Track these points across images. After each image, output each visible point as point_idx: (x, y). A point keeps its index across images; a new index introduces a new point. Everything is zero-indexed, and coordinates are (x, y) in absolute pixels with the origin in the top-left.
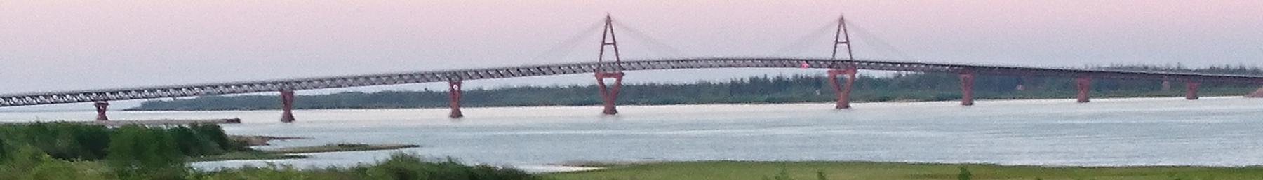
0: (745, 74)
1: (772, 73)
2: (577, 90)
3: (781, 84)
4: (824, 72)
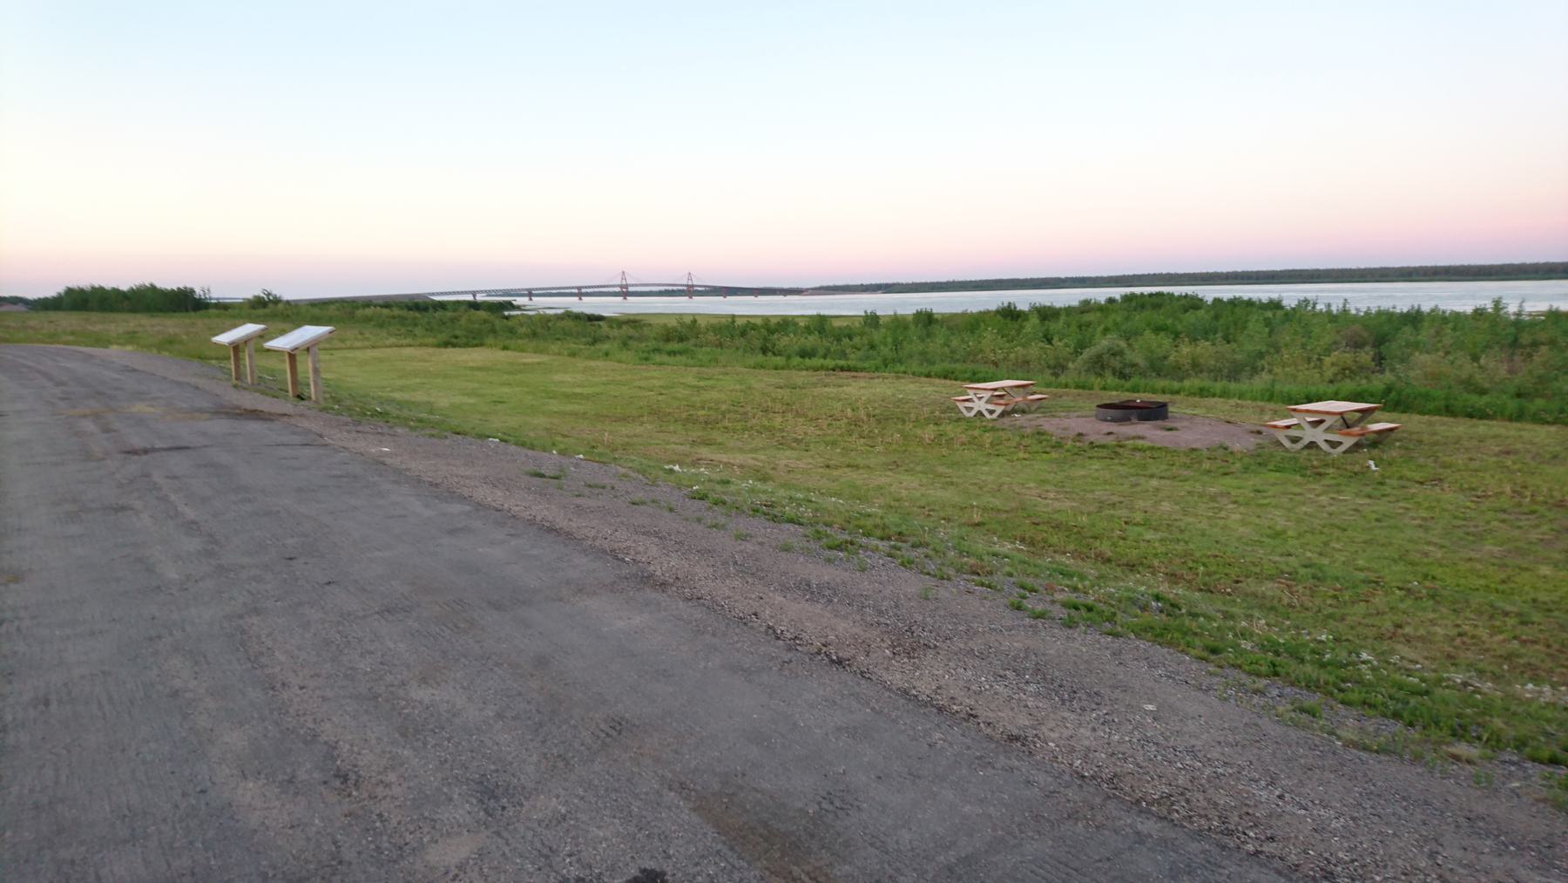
0: (663, 288)
1: (670, 288)
3: (673, 291)
4: (685, 288)
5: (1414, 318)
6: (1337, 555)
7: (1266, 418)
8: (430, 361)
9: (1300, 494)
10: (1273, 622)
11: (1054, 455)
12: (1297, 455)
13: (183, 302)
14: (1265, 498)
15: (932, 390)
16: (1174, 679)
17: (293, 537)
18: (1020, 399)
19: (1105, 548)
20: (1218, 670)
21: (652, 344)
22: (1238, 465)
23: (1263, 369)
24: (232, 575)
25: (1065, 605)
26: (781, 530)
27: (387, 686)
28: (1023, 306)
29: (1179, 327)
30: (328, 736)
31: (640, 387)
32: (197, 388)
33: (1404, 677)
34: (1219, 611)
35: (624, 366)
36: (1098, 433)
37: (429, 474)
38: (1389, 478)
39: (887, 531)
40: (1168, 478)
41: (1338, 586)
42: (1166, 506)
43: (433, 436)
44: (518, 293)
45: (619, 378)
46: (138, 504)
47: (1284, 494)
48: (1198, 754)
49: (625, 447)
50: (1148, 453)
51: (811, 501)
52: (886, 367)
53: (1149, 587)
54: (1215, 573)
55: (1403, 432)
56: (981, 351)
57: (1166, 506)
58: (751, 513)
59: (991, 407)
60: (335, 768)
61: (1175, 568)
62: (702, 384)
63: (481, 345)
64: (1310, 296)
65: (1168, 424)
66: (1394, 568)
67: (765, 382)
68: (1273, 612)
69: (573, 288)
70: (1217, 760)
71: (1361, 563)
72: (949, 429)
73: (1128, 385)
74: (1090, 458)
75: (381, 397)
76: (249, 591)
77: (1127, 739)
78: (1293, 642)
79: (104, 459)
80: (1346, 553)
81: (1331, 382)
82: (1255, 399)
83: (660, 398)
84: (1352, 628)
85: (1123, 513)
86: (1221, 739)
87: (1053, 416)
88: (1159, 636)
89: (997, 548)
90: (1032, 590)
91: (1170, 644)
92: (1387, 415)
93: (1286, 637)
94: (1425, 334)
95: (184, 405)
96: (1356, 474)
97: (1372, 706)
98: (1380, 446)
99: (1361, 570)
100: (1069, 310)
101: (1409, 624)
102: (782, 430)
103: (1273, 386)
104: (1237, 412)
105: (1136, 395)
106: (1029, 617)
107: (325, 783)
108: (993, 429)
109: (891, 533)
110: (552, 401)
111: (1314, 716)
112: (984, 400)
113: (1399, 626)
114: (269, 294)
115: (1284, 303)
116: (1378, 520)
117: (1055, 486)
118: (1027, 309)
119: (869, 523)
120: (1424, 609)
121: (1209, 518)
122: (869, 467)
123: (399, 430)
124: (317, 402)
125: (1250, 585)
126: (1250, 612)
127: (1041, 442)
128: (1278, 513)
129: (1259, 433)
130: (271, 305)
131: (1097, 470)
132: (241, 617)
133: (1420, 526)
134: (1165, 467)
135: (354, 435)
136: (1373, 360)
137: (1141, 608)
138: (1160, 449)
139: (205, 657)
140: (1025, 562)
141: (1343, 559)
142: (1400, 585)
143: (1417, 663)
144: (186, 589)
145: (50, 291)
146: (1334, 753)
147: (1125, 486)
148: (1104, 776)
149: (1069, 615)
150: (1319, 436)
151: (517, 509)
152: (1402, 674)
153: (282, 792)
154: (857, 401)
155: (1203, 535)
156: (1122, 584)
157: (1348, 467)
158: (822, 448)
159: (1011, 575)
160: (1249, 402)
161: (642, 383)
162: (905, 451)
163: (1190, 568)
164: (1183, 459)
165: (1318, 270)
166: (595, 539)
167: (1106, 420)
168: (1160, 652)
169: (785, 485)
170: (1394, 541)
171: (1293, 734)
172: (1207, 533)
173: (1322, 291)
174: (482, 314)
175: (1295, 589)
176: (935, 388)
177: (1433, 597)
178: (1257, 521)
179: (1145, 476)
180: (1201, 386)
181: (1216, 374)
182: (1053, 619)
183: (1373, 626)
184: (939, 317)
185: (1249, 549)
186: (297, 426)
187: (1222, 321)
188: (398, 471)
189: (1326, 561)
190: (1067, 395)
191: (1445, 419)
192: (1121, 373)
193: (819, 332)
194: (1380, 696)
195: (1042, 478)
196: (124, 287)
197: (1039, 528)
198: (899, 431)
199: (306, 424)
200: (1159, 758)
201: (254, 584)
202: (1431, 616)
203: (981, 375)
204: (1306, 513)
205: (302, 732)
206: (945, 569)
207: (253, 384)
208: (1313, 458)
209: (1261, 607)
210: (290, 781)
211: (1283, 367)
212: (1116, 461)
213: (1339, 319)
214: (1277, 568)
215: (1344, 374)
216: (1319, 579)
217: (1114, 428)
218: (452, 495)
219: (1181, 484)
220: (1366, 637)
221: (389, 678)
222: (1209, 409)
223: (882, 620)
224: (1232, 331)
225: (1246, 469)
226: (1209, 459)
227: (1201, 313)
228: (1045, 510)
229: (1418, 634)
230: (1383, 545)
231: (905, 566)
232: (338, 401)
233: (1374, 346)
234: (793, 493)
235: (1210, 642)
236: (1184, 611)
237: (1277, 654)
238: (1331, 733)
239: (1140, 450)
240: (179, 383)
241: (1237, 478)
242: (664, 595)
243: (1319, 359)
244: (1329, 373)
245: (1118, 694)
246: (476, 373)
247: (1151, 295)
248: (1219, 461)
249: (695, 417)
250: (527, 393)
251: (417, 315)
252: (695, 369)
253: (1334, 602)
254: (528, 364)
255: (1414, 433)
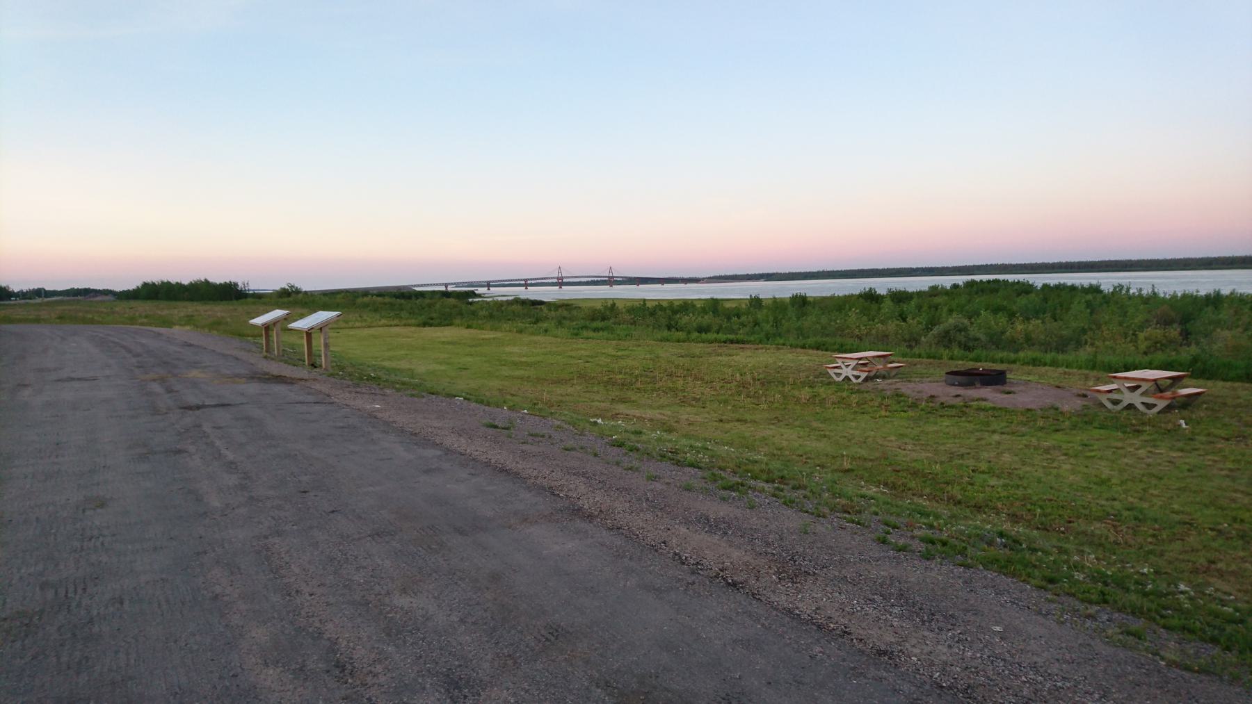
0: (590, 279)
1: (596, 279)
2: (553, 283)
3: (597, 281)
4: (607, 279)
5: (1215, 300)
6: (1155, 500)
7: (1091, 383)
8: (413, 337)
9: (1122, 448)
10: (1101, 556)
11: (911, 413)
12: (1118, 415)
13: (229, 293)
14: (1093, 451)
15: (807, 359)
16: (1017, 604)
17: (306, 475)
18: (881, 367)
19: (956, 491)
20: (1055, 597)
21: (581, 323)
22: (1067, 423)
23: (1086, 343)
24: (260, 504)
25: (923, 540)
26: (683, 473)
27: (376, 595)
28: (882, 291)
29: (1014, 308)
30: (330, 634)
31: (571, 357)
32: (237, 359)
33: (1219, 607)
34: (1055, 547)
35: (559, 340)
36: (948, 396)
37: (410, 426)
38: (1198, 434)
39: (771, 475)
40: (1008, 434)
41: (1157, 526)
42: (1007, 457)
43: (412, 395)
44: (480, 285)
45: (555, 349)
46: (192, 449)
47: (1108, 447)
48: (1041, 670)
49: (559, 404)
50: (990, 412)
51: (708, 449)
52: (768, 340)
53: (994, 525)
54: (1050, 514)
55: (1209, 395)
56: (848, 327)
57: (1007, 457)
58: (659, 458)
59: (856, 373)
60: (335, 659)
61: (1015, 510)
62: (619, 353)
63: (451, 325)
64: (1124, 282)
65: (1007, 388)
66: (1207, 512)
67: (670, 352)
68: (1101, 548)
69: (521, 280)
70: (1057, 675)
71: (1176, 507)
72: (823, 391)
73: (971, 355)
74: (941, 416)
75: (374, 365)
76: (273, 518)
77: (979, 655)
78: (1120, 575)
79: (166, 413)
80: (1163, 499)
81: (1145, 353)
82: (1080, 368)
83: (587, 365)
84: (1170, 563)
85: (971, 462)
86: (1060, 657)
87: (910, 381)
88: (1004, 567)
89: (864, 491)
90: (895, 527)
91: (1013, 575)
92: (1194, 381)
93: (1113, 569)
94: (1225, 314)
95: (228, 372)
96: (1169, 431)
97: (1191, 631)
98: (1190, 408)
99: (1177, 513)
100: (920, 294)
101: (1221, 560)
102: (683, 391)
103: (1095, 356)
104: (1065, 378)
105: (979, 364)
106: (892, 550)
107: (328, 671)
108: (859, 391)
109: (775, 477)
110: (504, 367)
111: (1140, 638)
112: (850, 367)
113: (1213, 562)
114: (293, 286)
115: (1102, 288)
116: (1189, 470)
117: (913, 439)
118: (885, 294)
119: (756, 468)
120: (1235, 548)
121: (1044, 467)
122: (755, 422)
123: (388, 391)
124: (326, 369)
125: (1081, 525)
126: (1081, 548)
127: (899, 403)
128: (1103, 464)
129: (1085, 396)
130: (293, 295)
131: (948, 426)
132: (266, 537)
133: (1228, 476)
134: (1004, 424)
135: (354, 395)
136: (1181, 334)
137: (987, 543)
138: (1000, 409)
139: (239, 568)
140: (888, 503)
141: (1161, 503)
142: (1211, 526)
143: (1231, 594)
144: (226, 515)
145: (132, 285)
146: (1159, 671)
147: (971, 440)
148: (959, 687)
149: (927, 548)
150: (1136, 399)
151: (477, 453)
152: (1217, 604)
153: (294, 678)
154: (744, 367)
155: (1039, 481)
156: (971, 522)
157: (1163, 425)
158: (716, 405)
159: (876, 514)
160: (1075, 370)
161: (573, 354)
162: (785, 409)
163: (1029, 510)
164: (1021, 418)
165: (1131, 261)
166: (536, 478)
167: (954, 385)
168: (1005, 581)
169: (687, 436)
170: (1204, 489)
171: (1122, 654)
172: (1042, 480)
173: (1037, 278)
174: (452, 301)
175: (1119, 529)
176: (810, 358)
177: (1242, 537)
178: (1085, 470)
179: (988, 431)
180: (1034, 356)
181: (1046, 347)
182: (913, 552)
183: (1189, 561)
184: (811, 300)
185: (1079, 494)
186: (311, 388)
187: (1050, 303)
188: (387, 423)
189: (1145, 505)
190: (921, 364)
191: (1247, 385)
192: (965, 346)
193: (713, 312)
194: (1198, 623)
195: (901, 432)
196: (186, 282)
197: (900, 474)
198: (780, 392)
199: (317, 386)
200: (1007, 672)
201: (276, 511)
202: (1242, 554)
203: (848, 347)
204: (1127, 464)
205: (310, 630)
206: (820, 508)
207: (278, 356)
208: (1131, 417)
209: (1091, 544)
210: (301, 669)
211: (1104, 341)
212: (963, 419)
213: (1151, 300)
214: (1104, 511)
215: (1156, 347)
216: (1140, 521)
217: (960, 391)
218: (427, 442)
219: (1020, 438)
220: (1183, 571)
221: (377, 588)
222: (1041, 376)
223: (769, 550)
224: (1058, 311)
225: (1074, 427)
226: (1042, 417)
227: (1033, 296)
228: (904, 459)
229: (1230, 570)
230: (1195, 492)
231: (787, 505)
232: (342, 368)
233: (1180, 323)
234: (692, 442)
235: (1048, 573)
236: (1024, 546)
237: (1105, 583)
238: (1155, 654)
239: (983, 410)
240: (224, 356)
241: (1066, 434)
242: (591, 525)
243: (1133, 334)
244: (1143, 347)
245: (969, 617)
246: (447, 346)
247: (989, 282)
248: (1051, 420)
249: (614, 380)
250: (485, 362)
251: (403, 301)
252: (614, 342)
253: (1154, 540)
254: (486, 339)
255: (1218, 397)
